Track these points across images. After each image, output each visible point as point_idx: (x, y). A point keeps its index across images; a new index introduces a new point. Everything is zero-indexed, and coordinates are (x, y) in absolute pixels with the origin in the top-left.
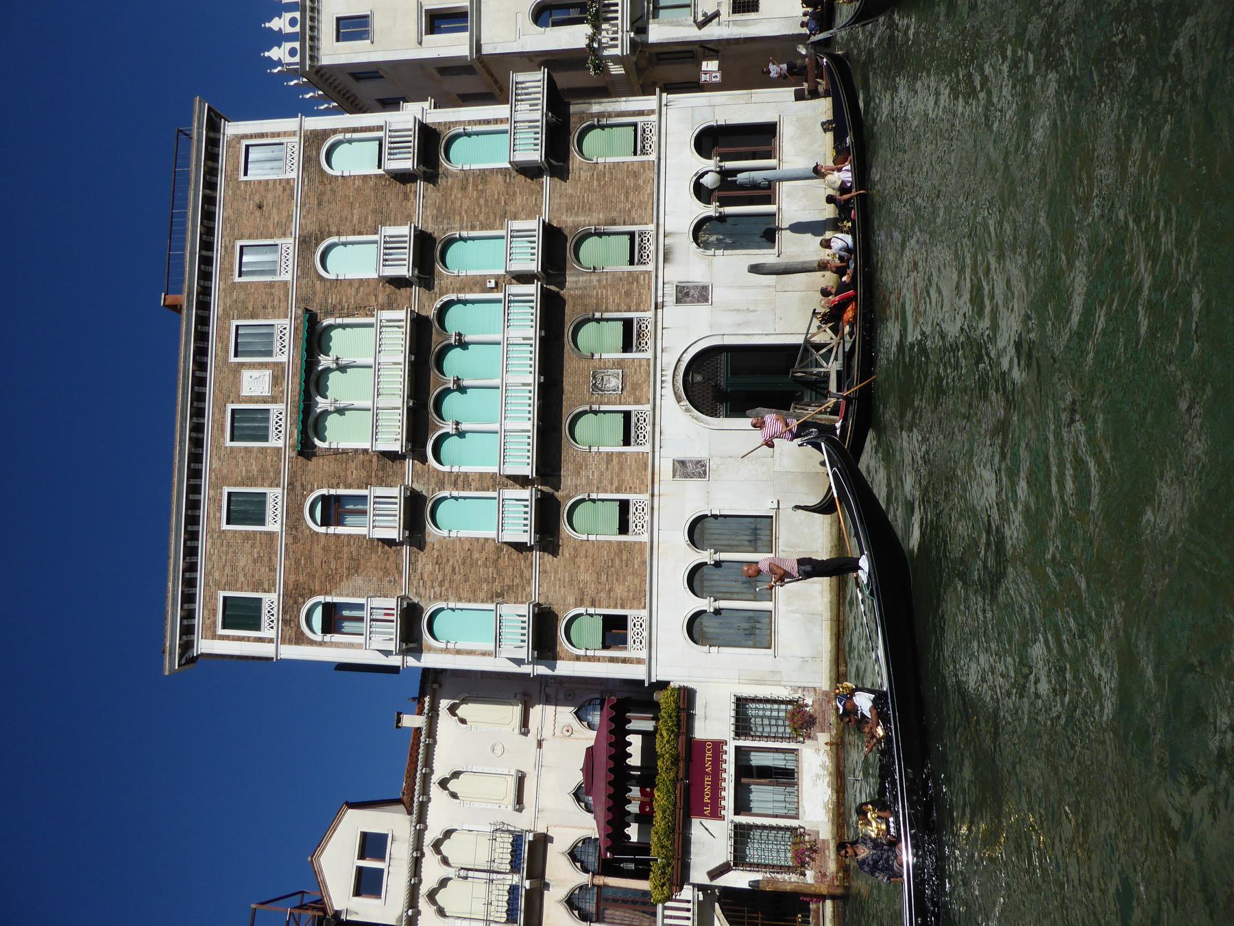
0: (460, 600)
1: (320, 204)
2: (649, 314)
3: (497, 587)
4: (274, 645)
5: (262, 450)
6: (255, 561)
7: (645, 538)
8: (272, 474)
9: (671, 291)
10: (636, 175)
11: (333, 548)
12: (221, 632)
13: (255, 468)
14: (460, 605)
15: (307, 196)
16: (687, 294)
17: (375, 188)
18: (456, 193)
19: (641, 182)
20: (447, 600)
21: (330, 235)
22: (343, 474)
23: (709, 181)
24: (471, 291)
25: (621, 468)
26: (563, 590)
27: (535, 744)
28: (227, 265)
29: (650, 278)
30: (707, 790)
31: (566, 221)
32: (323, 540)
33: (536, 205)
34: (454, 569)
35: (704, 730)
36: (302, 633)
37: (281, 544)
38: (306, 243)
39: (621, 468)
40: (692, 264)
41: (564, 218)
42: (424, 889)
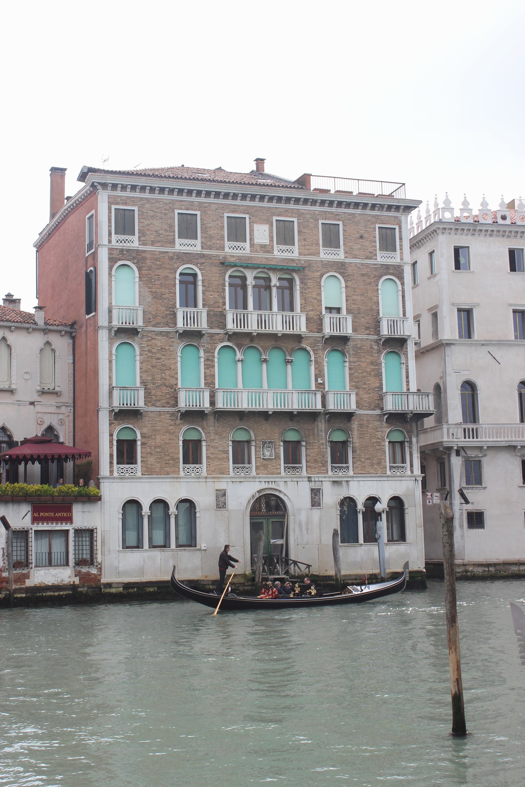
0: (141, 363)
1: (363, 275)
3: (150, 386)
4: (107, 243)
5: (223, 237)
6: (157, 231)
7: (182, 474)
8: (209, 243)
10: (379, 463)
11: (168, 282)
12: (113, 207)
13: (212, 232)
14: (138, 363)
15: (368, 267)
16: (316, 495)
17: (371, 309)
18: (369, 359)
19: (375, 466)
20: (141, 355)
21: (346, 281)
22: (211, 289)
23: (378, 507)
24: (316, 368)
25: (220, 459)
26: (150, 425)
27: (32, 400)
28: (328, 216)
29: (324, 473)
30: (47, 514)
31: (355, 425)
32: (171, 276)
33: (363, 406)
34: (159, 359)
36: (116, 262)
38: (340, 268)
39: (220, 459)
40: (331, 497)
41: (356, 423)
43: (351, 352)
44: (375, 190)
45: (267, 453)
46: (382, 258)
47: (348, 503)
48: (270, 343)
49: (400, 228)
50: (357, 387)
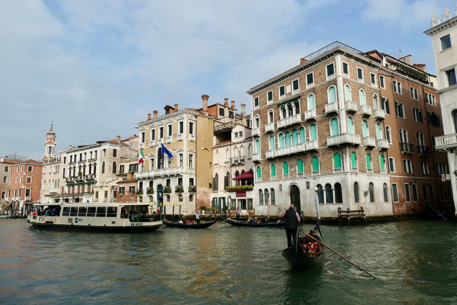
2: (304, 176)
7: (271, 180)
9: (308, 180)
31: (320, 154)
35: (247, 193)
37: (266, 106)
38: (313, 90)
42: (236, 145)
44: (322, 52)
45: (292, 170)
46: (328, 79)
47: (319, 186)
48: (292, 128)
50: (321, 138)
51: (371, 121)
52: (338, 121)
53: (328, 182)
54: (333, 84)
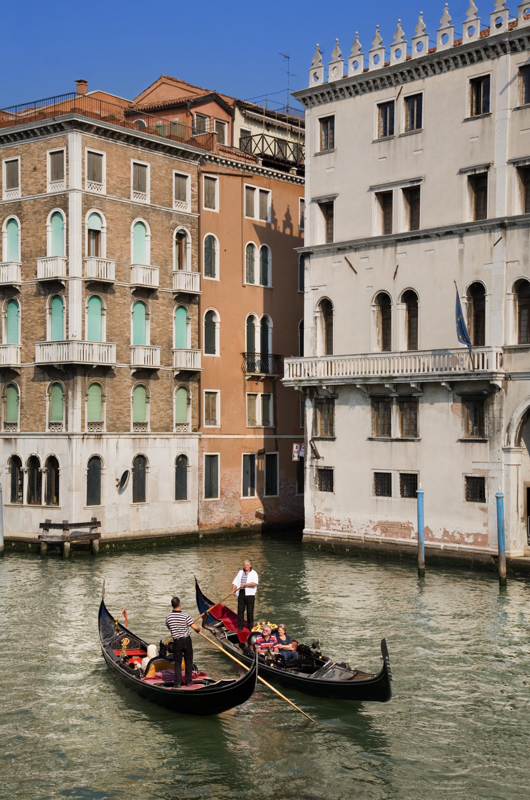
1: (35, 213)
19: (38, 423)
38: (17, 207)
41: (25, 377)
43: (23, 301)
46: (50, 189)
49: (67, 150)
50: (27, 338)
51: (161, 300)
52: (65, 306)
53: (34, 453)
54: (59, 206)
